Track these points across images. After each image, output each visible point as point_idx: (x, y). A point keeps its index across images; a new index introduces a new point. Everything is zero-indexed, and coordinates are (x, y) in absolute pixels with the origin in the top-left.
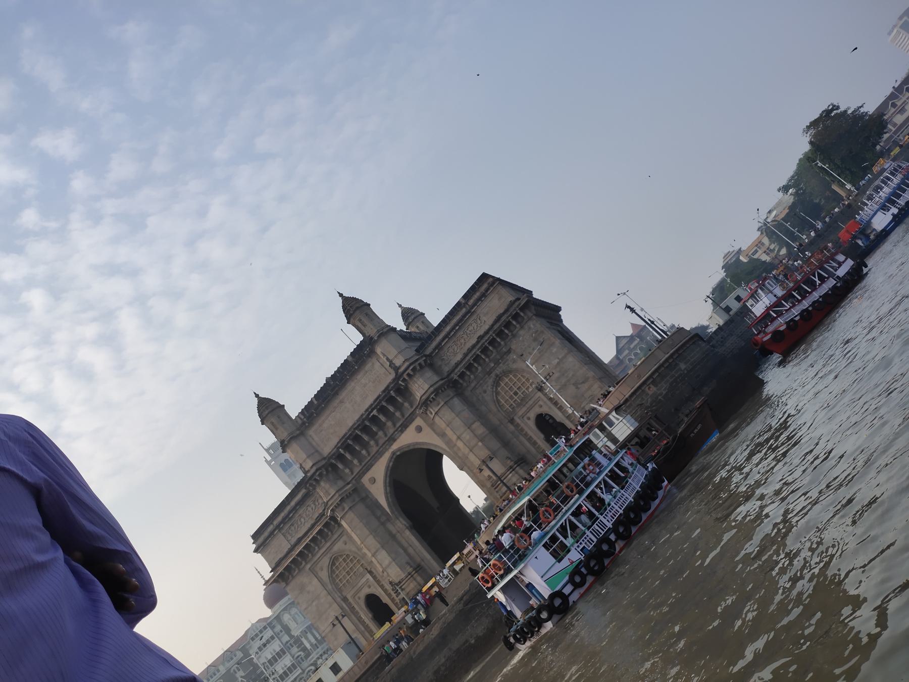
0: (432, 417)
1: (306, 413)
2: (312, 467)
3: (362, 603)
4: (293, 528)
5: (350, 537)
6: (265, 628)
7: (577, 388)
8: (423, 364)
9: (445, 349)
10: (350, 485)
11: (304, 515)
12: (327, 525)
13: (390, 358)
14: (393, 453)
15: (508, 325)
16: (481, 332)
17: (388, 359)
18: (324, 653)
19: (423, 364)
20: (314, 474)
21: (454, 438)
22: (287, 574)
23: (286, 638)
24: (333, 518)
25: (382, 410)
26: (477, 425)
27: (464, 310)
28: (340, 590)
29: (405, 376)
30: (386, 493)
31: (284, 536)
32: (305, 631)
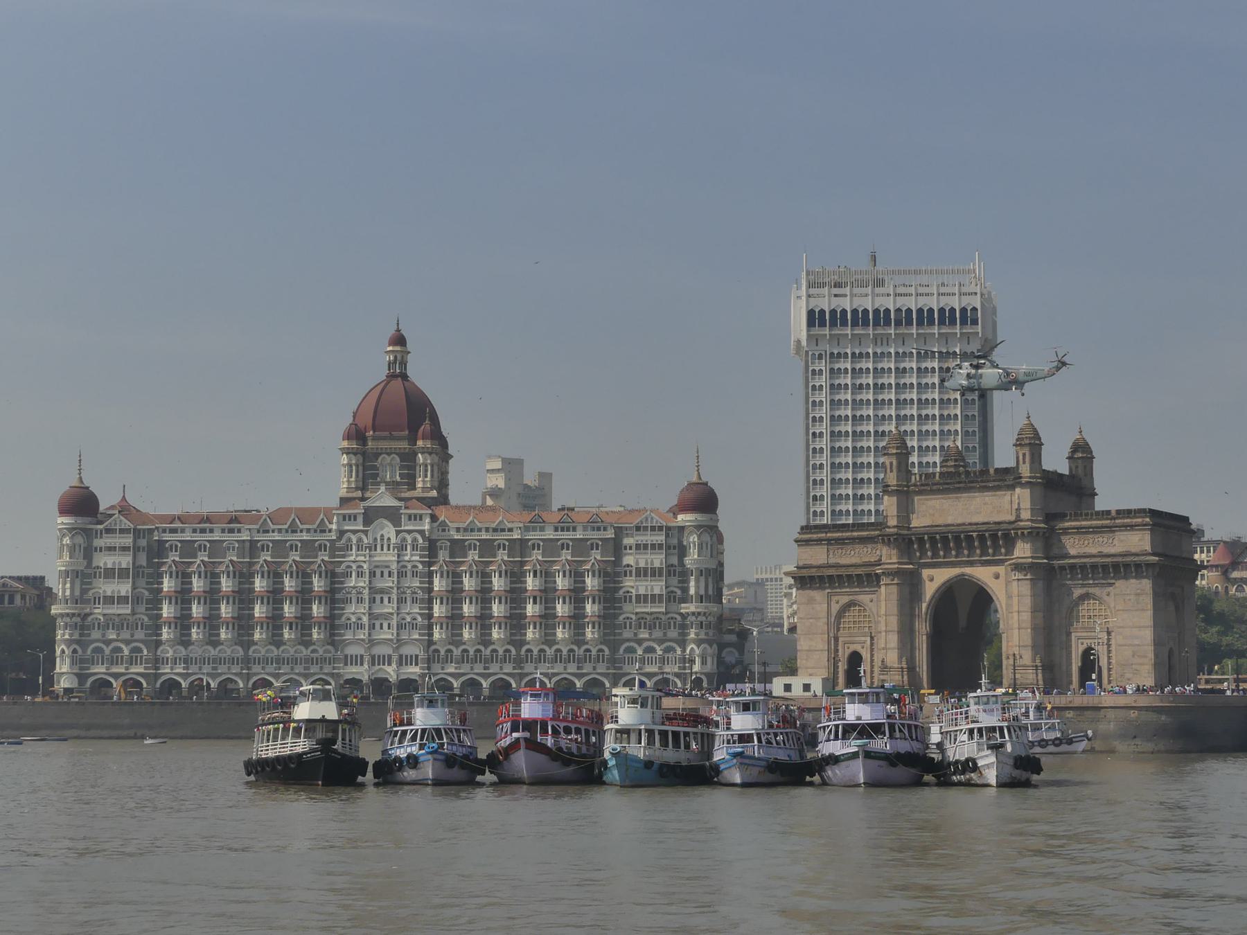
0: (1014, 578)
1: (923, 478)
2: (894, 527)
3: (848, 652)
4: (840, 551)
5: (879, 601)
6: (660, 528)
7: (1133, 656)
8: (1041, 534)
9: (1068, 537)
10: (911, 566)
11: (857, 550)
12: (869, 575)
13: (1022, 506)
14: (963, 575)
15: (1127, 566)
16: (1106, 550)
17: (1019, 504)
18: (705, 613)
19: (1041, 534)
20: (892, 535)
21: (1016, 608)
22: (808, 581)
23: (675, 561)
24: (878, 577)
25: (982, 538)
26: (1040, 615)
27: (1108, 522)
28: (838, 629)
29: (1019, 532)
30: (933, 597)
31: (828, 551)
32: (702, 571)
